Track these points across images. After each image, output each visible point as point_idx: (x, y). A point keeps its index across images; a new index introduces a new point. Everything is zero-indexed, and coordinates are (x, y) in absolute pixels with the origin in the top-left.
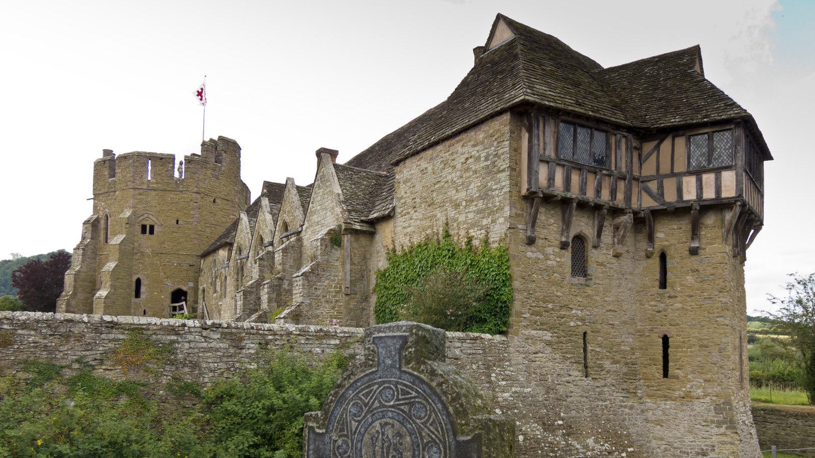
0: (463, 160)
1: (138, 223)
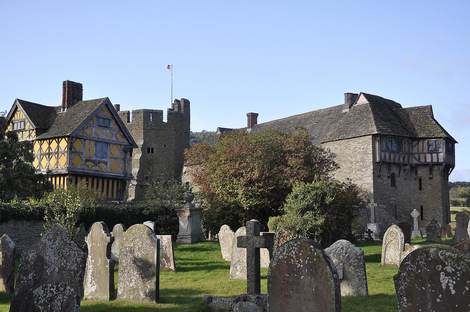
0: (354, 148)
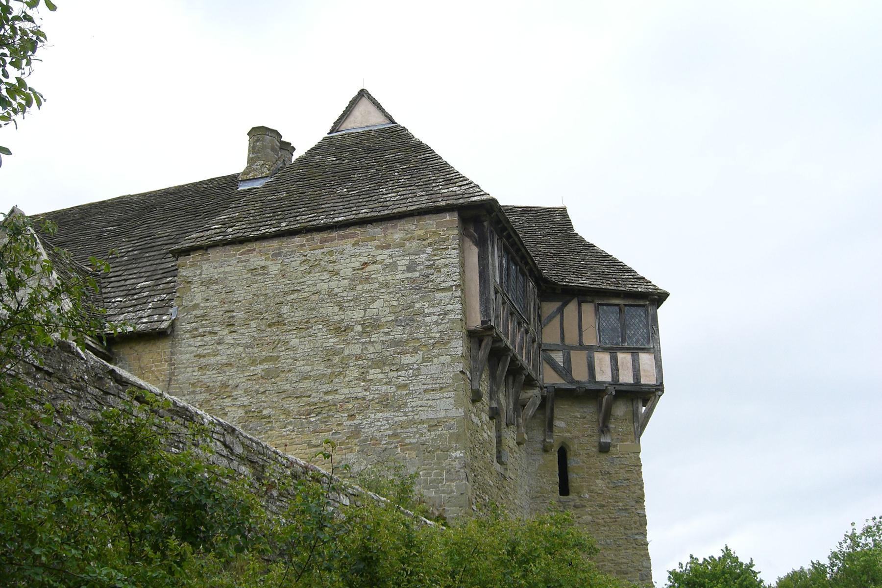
0: (357, 265)
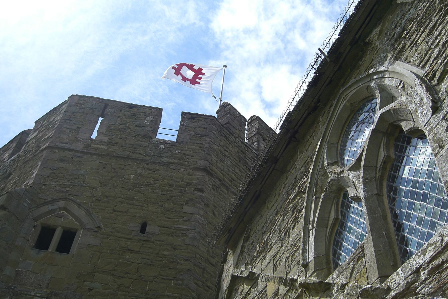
1: (36, 220)
